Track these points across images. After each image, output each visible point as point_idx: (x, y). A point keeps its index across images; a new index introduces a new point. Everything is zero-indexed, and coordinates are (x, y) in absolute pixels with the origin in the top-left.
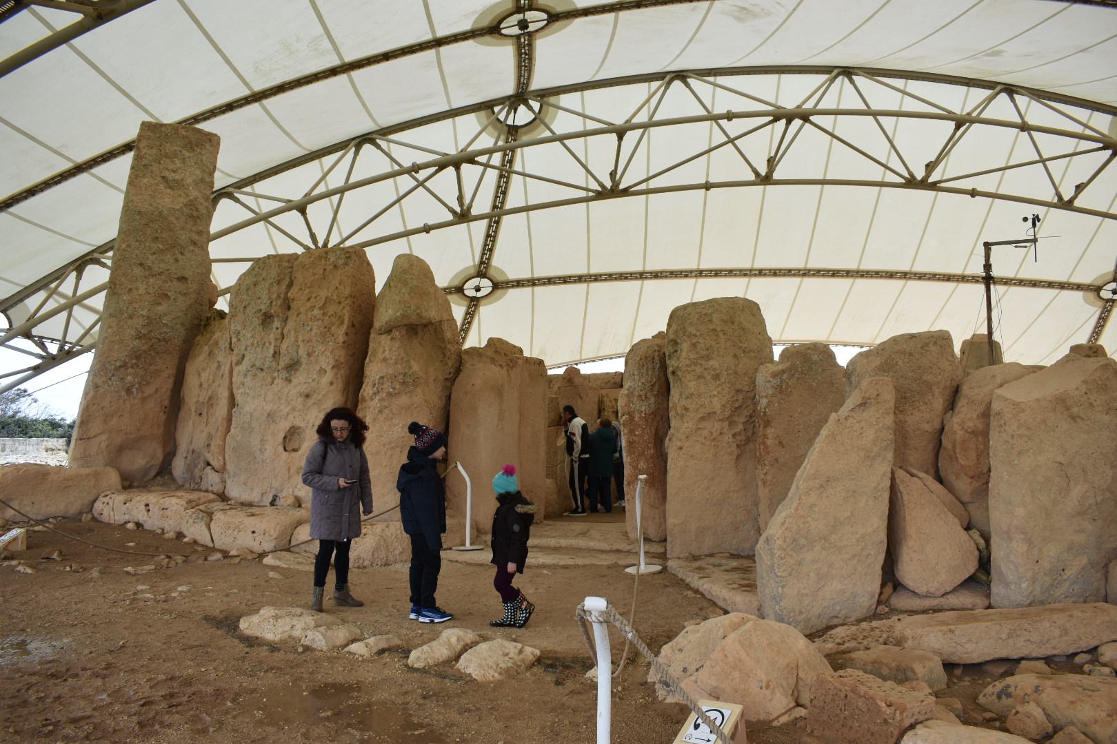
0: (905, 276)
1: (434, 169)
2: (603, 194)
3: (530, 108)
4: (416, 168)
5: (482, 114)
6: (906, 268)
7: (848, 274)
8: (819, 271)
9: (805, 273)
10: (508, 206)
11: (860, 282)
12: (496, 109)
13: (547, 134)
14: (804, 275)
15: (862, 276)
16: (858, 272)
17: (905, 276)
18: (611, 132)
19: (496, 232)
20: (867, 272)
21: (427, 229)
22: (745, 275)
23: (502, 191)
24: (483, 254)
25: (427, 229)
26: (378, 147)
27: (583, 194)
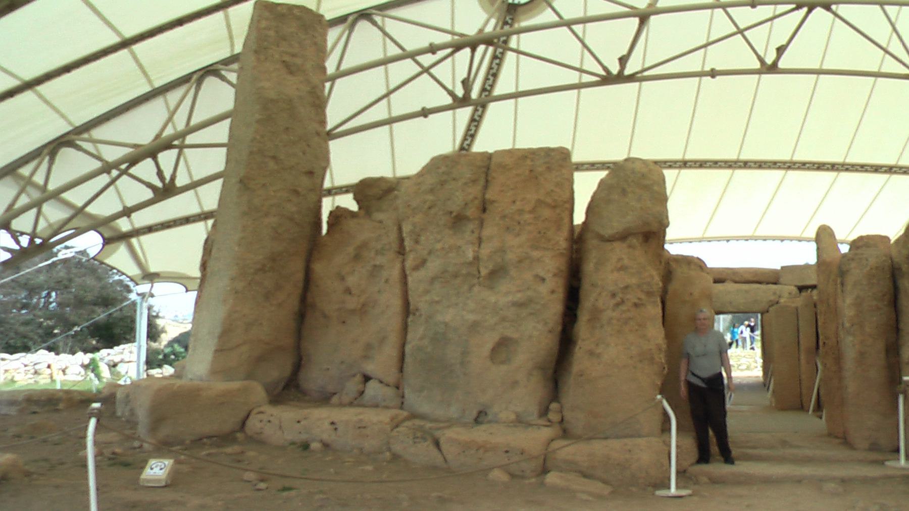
0: (890, 170)
2: (608, 79)
4: (432, 49)
6: (892, 162)
7: (833, 167)
8: (804, 164)
9: (790, 166)
10: (497, 92)
11: (844, 175)
14: (789, 168)
15: (847, 170)
16: (843, 165)
17: (890, 170)
18: (634, 16)
19: (481, 117)
20: (853, 165)
21: (425, 113)
22: (730, 167)
23: (493, 74)
24: (465, 139)
25: (425, 113)
26: (375, 23)
27: (573, 78)
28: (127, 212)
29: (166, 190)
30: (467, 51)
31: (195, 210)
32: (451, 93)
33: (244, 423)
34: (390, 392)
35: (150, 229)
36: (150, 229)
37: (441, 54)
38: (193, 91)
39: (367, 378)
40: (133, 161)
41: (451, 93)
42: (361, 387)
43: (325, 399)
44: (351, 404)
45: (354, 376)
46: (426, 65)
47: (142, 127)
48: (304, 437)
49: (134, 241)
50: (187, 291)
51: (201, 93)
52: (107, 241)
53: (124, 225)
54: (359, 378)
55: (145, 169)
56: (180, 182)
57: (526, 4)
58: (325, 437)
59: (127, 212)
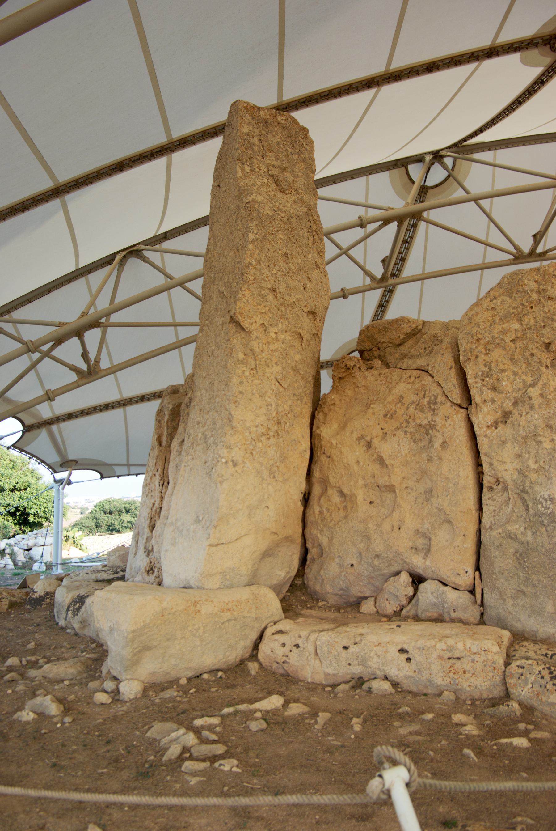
1: (381, 222)
3: (445, 167)
5: (398, 172)
12: (410, 167)
13: (460, 193)
28: (49, 396)
29: (90, 373)
30: (395, 224)
31: (114, 397)
32: (367, 273)
33: (256, 646)
34: (464, 598)
35: (70, 416)
36: (70, 416)
37: (371, 227)
38: (116, 272)
39: (417, 580)
40: (59, 341)
41: (367, 273)
42: (410, 591)
43: (350, 608)
44: (397, 615)
45: (397, 573)
46: (345, 245)
47: (68, 306)
48: (357, 670)
49: (54, 427)
50: (102, 477)
51: (123, 275)
52: (27, 429)
53: (45, 411)
54: (405, 578)
55: (71, 350)
56: (104, 364)
57: (437, 186)
58: (393, 672)
59: (49, 396)
